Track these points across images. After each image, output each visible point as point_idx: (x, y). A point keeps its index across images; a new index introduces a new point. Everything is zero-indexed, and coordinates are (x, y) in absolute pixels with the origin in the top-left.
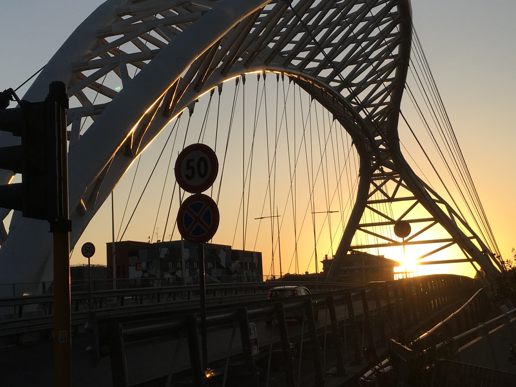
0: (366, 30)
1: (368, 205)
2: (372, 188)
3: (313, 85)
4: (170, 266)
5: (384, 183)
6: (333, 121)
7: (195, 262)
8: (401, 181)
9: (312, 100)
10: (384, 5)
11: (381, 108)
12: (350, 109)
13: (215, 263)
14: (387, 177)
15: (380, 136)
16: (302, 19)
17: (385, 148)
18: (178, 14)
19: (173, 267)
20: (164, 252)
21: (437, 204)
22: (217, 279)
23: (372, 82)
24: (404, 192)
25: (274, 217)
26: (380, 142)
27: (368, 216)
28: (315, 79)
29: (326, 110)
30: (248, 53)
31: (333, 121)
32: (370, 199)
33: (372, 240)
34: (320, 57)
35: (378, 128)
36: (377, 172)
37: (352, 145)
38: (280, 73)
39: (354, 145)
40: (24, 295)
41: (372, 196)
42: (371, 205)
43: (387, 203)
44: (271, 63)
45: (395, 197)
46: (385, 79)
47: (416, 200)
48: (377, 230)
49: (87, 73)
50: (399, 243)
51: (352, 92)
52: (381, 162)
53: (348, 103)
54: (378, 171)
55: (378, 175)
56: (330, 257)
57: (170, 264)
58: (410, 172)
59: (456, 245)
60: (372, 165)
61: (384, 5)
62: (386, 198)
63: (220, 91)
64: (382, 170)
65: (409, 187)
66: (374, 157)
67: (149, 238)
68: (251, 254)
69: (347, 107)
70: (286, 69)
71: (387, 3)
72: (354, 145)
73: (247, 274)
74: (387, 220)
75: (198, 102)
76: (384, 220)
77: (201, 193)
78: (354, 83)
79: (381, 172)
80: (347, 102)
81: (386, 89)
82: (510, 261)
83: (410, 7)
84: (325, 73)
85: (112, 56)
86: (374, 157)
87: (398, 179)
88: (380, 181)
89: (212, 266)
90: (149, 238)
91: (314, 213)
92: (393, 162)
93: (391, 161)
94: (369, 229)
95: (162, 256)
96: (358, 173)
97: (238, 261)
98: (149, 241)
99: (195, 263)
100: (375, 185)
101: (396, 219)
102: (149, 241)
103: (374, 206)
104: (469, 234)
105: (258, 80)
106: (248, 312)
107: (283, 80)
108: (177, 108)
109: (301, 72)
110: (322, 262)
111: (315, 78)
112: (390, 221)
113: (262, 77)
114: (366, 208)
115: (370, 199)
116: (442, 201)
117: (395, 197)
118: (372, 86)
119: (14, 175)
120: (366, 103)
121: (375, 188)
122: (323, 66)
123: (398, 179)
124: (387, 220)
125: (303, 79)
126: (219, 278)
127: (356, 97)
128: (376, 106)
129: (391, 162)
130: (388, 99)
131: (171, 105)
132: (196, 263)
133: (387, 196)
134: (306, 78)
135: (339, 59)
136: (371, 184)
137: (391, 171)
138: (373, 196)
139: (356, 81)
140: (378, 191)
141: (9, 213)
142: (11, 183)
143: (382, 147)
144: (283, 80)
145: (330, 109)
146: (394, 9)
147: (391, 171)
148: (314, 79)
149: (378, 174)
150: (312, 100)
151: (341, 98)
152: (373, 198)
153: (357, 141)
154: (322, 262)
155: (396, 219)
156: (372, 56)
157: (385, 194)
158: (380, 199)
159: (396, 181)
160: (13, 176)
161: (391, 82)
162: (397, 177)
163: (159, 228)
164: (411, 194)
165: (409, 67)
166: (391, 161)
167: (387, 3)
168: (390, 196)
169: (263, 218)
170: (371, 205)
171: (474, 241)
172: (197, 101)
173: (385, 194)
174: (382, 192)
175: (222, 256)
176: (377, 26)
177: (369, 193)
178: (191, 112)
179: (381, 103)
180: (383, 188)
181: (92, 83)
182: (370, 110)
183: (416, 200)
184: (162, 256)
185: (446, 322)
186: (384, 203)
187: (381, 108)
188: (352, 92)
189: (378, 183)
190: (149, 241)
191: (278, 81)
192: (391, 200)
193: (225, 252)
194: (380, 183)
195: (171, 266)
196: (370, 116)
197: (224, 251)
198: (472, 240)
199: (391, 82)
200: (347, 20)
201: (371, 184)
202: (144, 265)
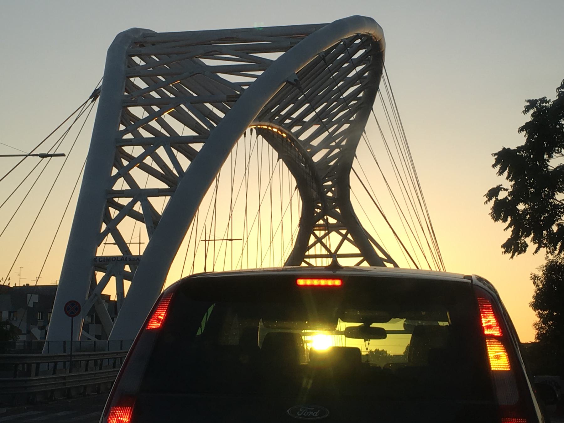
1: (305, 259)
2: (312, 240)
3: (277, 132)
4: (38, 318)
6: (278, 161)
7: (40, 312)
8: (347, 234)
9: (257, 136)
13: (95, 316)
14: (329, 228)
16: (303, 95)
18: (158, 60)
19: (42, 319)
20: (33, 299)
21: (384, 262)
22: (95, 337)
24: (349, 248)
26: (329, 189)
28: (281, 128)
30: (230, 108)
32: (307, 253)
35: (330, 173)
36: (321, 222)
41: (310, 250)
42: (307, 260)
45: (339, 253)
47: (362, 258)
52: (327, 211)
55: (320, 226)
57: (39, 315)
58: (359, 225)
60: (315, 214)
62: (328, 253)
65: (356, 243)
69: (302, 152)
70: (261, 122)
72: (297, 190)
80: (302, 147)
83: (384, 56)
86: (320, 205)
89: (90, 321)
93: (338, 210)
98: (9, 283)
99: (38, 313)
100: (315, 236)
102: (9, 284)
109: (271, 122)
111: (280, 125)
115: (307, 253)
116: (390, 260)
117: (338, 253)
119: (99, 246)
121: (316, 240)
123: (344, 232)
126: (97, 337)
129: (337, 212)
130: (344, 143)
132: (40, 313)
134: (272, 128)
136: (312, 236)
138: (313, 248)
140: (319, 244)
141: (109, 280)
143: (330, 194)
148: (278, 127)
150: (257, 136)
152: (311, 252)
153: (302, 186)
159: (340, 234)
160: (98, 248)
163: (22, 267)
164: (357, 251)
165: (372, 111)
166: (338, 210)
168: (333, 251)
170: (307, 260)
183: (362, 258)
184: (31, 305)
189: (320, 233)
190: (8, 283)
191: (251, 134)
193: (107, 304)
195: (40, 318)
197: (106, 302)
200: (350, 109)
201: (312, 236)
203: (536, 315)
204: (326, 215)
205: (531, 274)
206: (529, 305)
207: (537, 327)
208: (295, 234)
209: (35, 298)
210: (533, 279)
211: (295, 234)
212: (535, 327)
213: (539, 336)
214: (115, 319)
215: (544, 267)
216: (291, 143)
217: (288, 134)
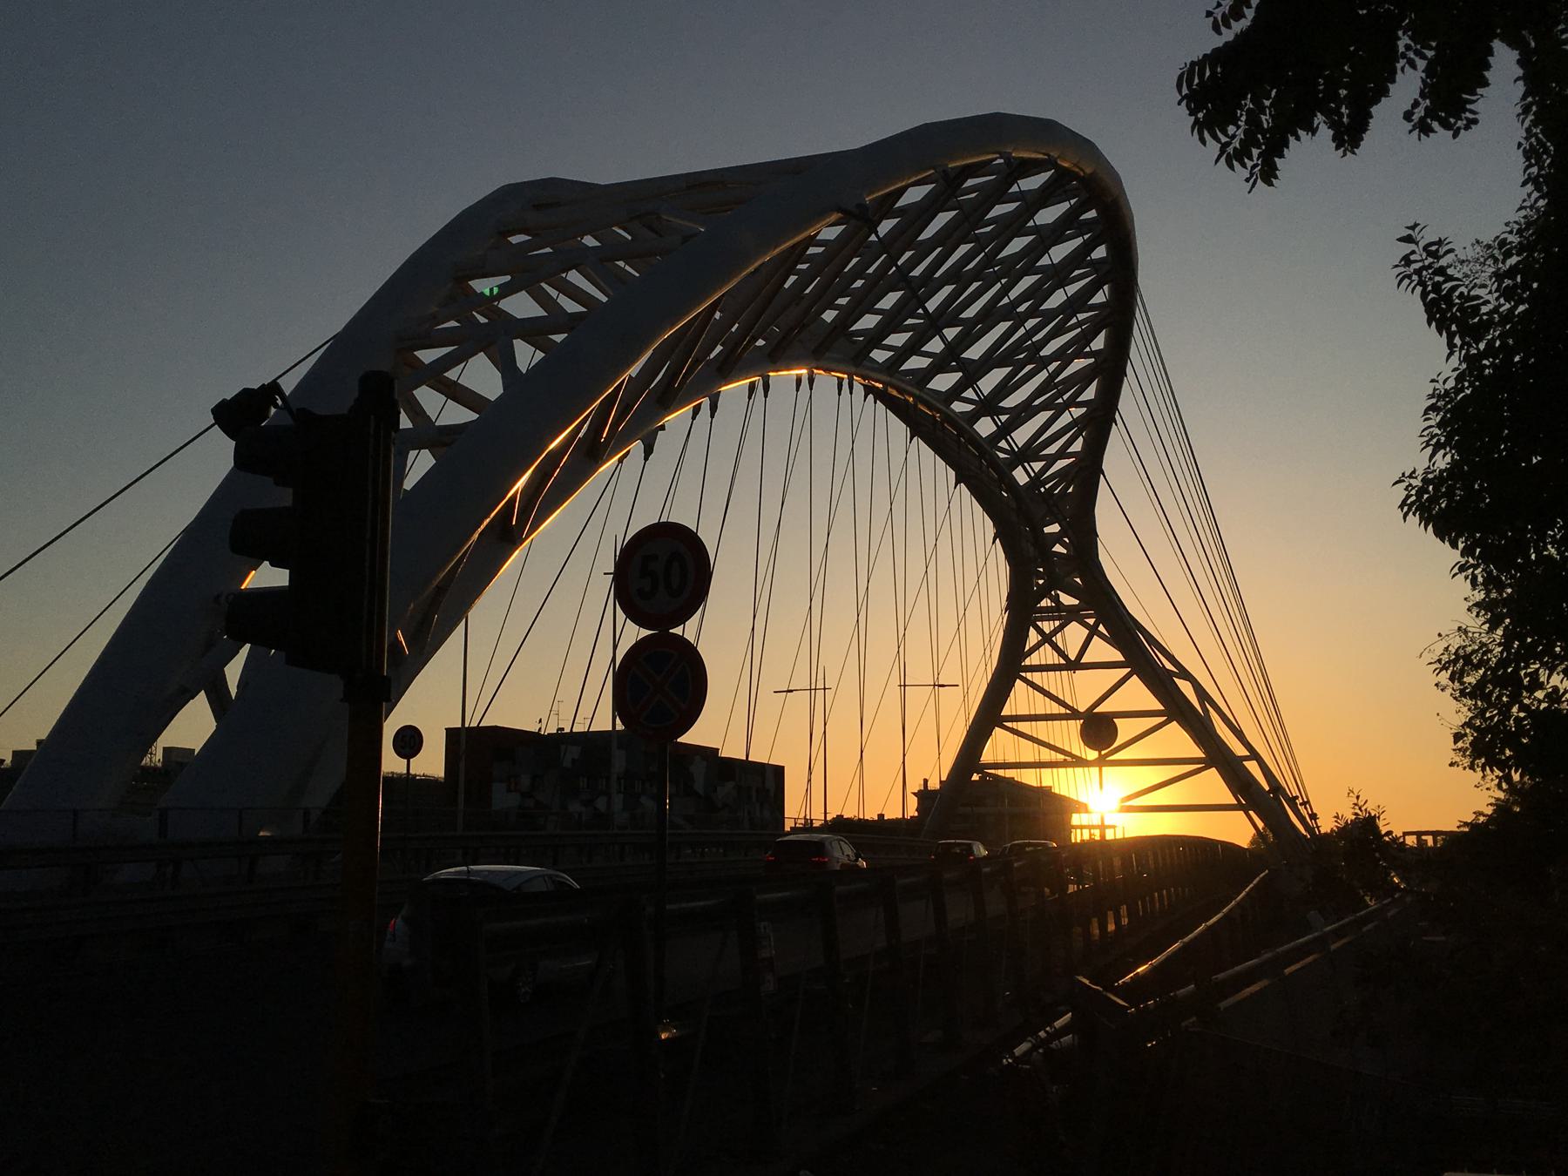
0: (1037, 294)
1: (1023, 674)
2: (1033, 638)
3: (915, 405)
5: (1061, 628)
6: (955, 488)
8: (1096, 625)
9: (911, 440)
10: (1079, 241)
11: (1061, 464)
12: (994, 463)
14: (1069, 615)
15: (1057, 524)
16: (899, 263)
17: (1065, 551)
18: (630, 238)
20: (571, 754)
23: (1044, 407)
24: (1102, 650)
25: (815, 689)
26: (1056, 538)
27: (1020, 699)
28: (922, 394)
29: (941, 462)
31: (955, 488)
32: (1027, 662)
33: (1028, 752)
34: (935, 345)
36: (1045, 603)
37: (994, 542)
38: (846, 376)
39: (998, 540)
40: (261, 834)
42: (1029, 676)
43: (1064, 673)
44: (827, 354)
46: (1072, 403)
47: (1127, 670)
48: (1040, 729)
49: (427, 356)
50: (1086, 760)
51: (1000, 424)
52: (1056, 582)
53: (989, 449)
54: (1049, 601)
55: (1047, 609)
56: (934, 784)
59: (1213, 772)
61: (1079, 241)
62: (1062, 661)
63: (713, 408)
64: (1056, 599)
65: (1115, 640)
66: (1041, 570)
67: (540, 721)
68: (761, 768)
71: (1086, 237)
72: (998, 540)
73: (749, 813)
74: (1063, 710)
75: (664, 429)
76: (1057, 709)
77: (671, 631)
78: (1003, 407)
79: (1053, 605)
81: (1075, 423)
82: (1342, 816)
84: (943, 382)
85: (483, 320)
86: (1041, 570)
87: (1091, 621)
88: (1051, 622)
90: (540, 721)
91: (905, 686)
92: (1080, 582)
93: (1078, 580)
94: (1023, 727)
95: (567, 763)
96: (1004, 603)
97: (730, 785)
98: (540, 729)
100: (1040, 631)
101: (1082, 709)
102: (540, 729)
103: (1036, 677)
104: (1240, 751)
105: (797, 390)
106: (758, 897)
107: (851, 393)
108: (619, 441)
109: (891, 376)
110: (914, 794)
111: (920, 390)
112: (1068, 712)
113: (805, 382)
114: (1018, 680)
115: (1027, 662)
116: (1186, 675)
118: (1044, 416)
120: (1028, 453)
121: (1040, 638)
122: (940, 365)
123: (1091, 621)
124: (1063, 710)
125: (895, 393)
127: (1008, 437)
128: (1051, 460)
130: (1077, 446)
131: (604, 436)
133: (1065, 657)
135: (975, 352)
136: (1032, 631)
137: (1077, 602)
139: (1009, 402)
140: (1046, 644)
141: (238, 652)
142: (251, 587)
143: (1058, 548)
144: (851, 393)
145: (950, 462)
146: (1100, 252)
147: (1077, 602)
148: (917, 392)
149: (1047, 607)
150: (911, 440)
151: (974, 438)
153: (1005, 534)
154: (914, 794)
155: (1082, 709)
156: (1047, 351)
157: (1061, 653)
158: (1050, 662)
159: (1086, 625)
160: (254, 572)
161: (1086, 409)
162: (1090, 616)
164: (1118, 657)
166: (1078, 580)
167: (1086, 237)
169: (791, 691)
170: (1029, 676)
171: (1252, 766)
172: (662, 428)
173: (1061, 653)
174: (1055, 647)
175: (698, 769)
176: (1062, 284)
177: (1027, 648)
178: (648, 451)
179: (1062, 454)
180: (1058, 639)
181: (435, 377)
182: (1037, 466)
183: (1127, 670)
184: (567, 763)
185: (1191, 940)
186: (1058, 673)
187: (1061, 464)
188: (1000, 424)
189: (1047, 627)
191: (840, 394)
192: (1074, 665)
194: (1052, 628)
196: (1036, 480)
198: (1246, 763)
199: (1086, 409)
200: (996, 269)
201: (1032, 631)
202: (525, 781)
203: (1462, 569)
204: (1055, 589)
205: (1408, 239)
206: (1400, 493)
207: (1471, 679)
208: (998, 627)
209: (573, 752)
210: (1418, 272)
211: (998, 627)
212: (1456, 677)
213: (1516, 50)
214: (718, 788)
215: (1508, 255)
216: (959, 435)
217: (945, 413)
